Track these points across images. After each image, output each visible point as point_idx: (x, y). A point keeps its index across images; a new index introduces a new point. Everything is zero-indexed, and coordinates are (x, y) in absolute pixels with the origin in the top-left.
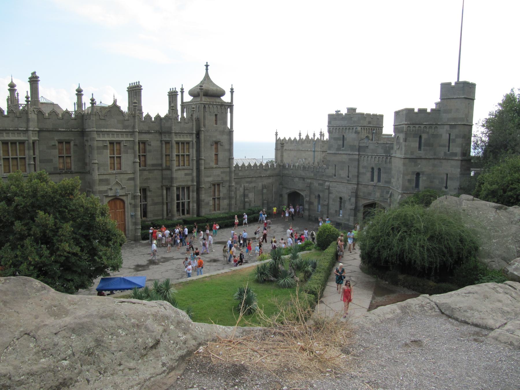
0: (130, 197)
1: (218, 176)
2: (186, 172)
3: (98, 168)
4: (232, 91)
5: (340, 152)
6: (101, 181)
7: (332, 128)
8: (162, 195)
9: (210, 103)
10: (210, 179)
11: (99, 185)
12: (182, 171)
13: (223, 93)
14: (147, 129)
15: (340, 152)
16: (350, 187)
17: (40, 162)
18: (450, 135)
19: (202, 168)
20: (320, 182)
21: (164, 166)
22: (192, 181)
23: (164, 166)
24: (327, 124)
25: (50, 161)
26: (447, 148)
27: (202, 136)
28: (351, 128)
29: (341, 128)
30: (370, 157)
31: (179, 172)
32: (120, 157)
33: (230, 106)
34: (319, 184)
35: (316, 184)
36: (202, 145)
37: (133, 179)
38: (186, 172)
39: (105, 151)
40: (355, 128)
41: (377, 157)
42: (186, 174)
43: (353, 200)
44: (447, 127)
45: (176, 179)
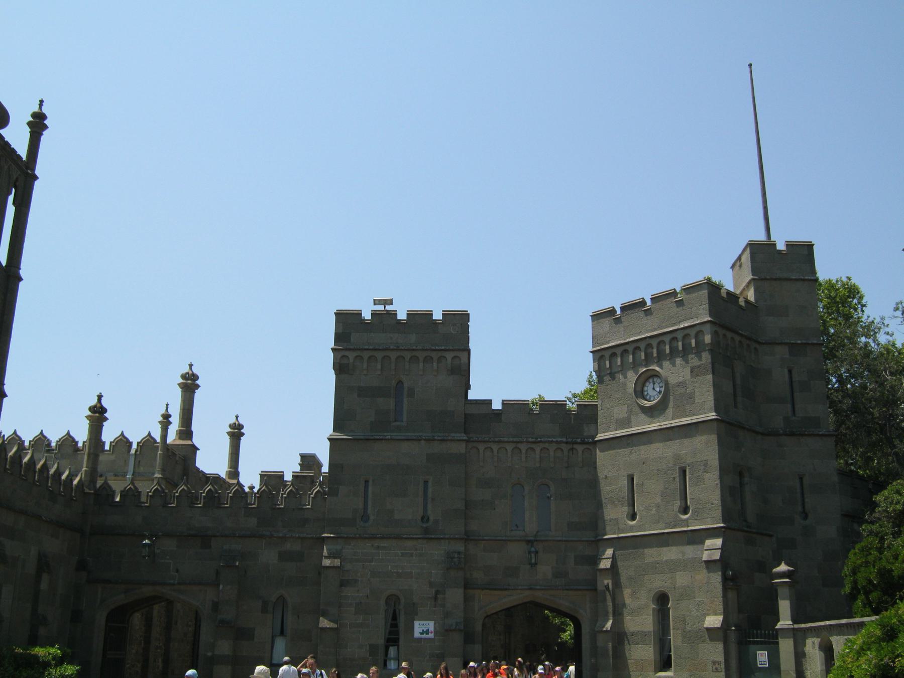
5: (388, 435)
7: (351, 355)
15: (388, 435)
16: (437, 551)
18: (790, 372)
20: (288, 546)
24: (330, 341)
26: (789, 406)
28: (435, 355)
29: (393, 355)
30: (510, 447)
34: (284, 556)
35: (268, 556)
40: (449, 356)
41: (538, 449)
43: (455, 596)
44: (781, 352)
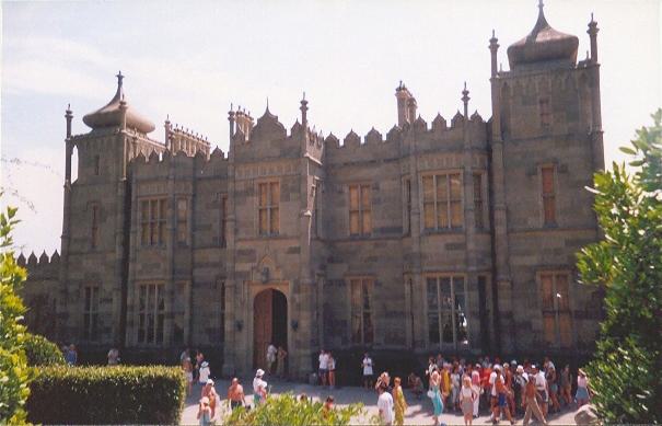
0: (291, 285)
1: (557, 252)
2: (450, 239)
3: (236, 231)
4: (593, 30)
6: (241, 252)
8: (403, 297)
9: (551, 76)
10: (533, 260)
11: (235, 260)
12: (440, 238)
13: (572, 43)
14: (372, 158)
17: (194, 229)
19: (500, 230)
21: (405, 229)
22: (467, 262)
23: (405, 229)
25: (209, 227)
27: (498, 156)
31: (432, 239)
32: (277, 209)
33: (591, 67)
36: (498, 177)
37: (296, 251)
38: (450, 239)
39: (250, 198)
42: (449, 247)
45: (422, 256)
